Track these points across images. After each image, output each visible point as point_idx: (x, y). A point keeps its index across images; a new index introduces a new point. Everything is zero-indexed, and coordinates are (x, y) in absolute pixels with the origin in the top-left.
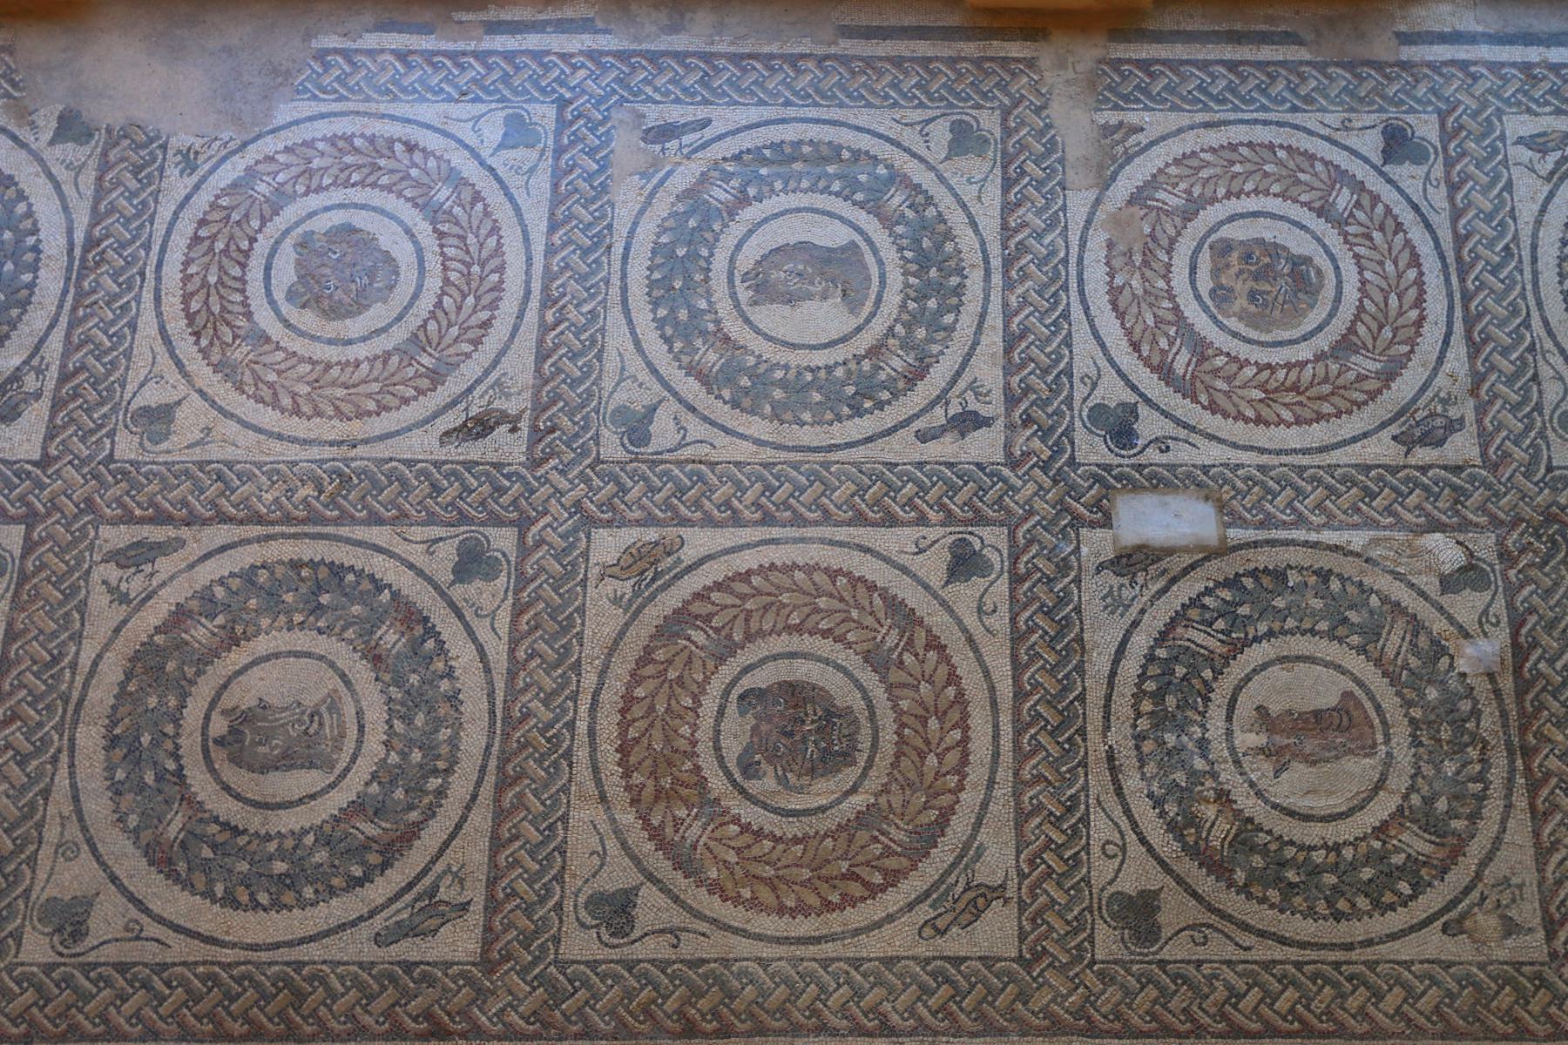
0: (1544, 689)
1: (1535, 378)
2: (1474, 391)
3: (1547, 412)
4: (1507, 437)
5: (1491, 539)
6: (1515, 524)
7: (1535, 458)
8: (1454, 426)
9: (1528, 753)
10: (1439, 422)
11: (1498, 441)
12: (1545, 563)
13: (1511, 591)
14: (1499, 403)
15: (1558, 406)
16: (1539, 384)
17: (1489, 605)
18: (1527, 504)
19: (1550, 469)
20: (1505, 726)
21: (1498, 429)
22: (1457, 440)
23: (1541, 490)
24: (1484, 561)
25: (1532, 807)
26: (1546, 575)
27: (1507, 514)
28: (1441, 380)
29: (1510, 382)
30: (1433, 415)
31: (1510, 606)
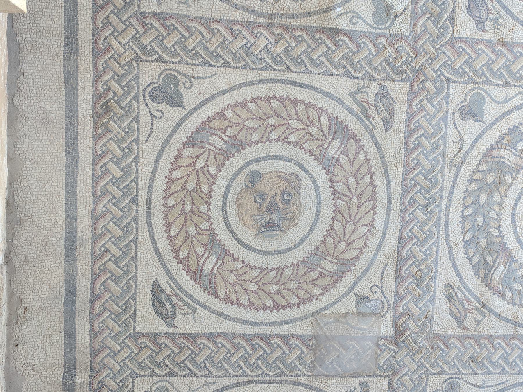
0: (309, 46)
1: (507, 84)
2: (501, 42)
3: (485, 87)
4: (471, 57)
5: (406, 32)
6: (414, 50)
7: (455, 72)
8: (480, 23)
9: (269, 26)
10: (484, 14)
11: (468, 51)
12: (388, 64)
13: (373, 38)
14: (493, 57)
15: (489, 95)
16: (503, 86)
17: (364, 21)
18: (427, 60)
19: (448, 80)
20: (287, 16)
21: (476, 52)
22: (472, 24)
23: (435, 72)
24: (392, 23)
25: (237, 22)
26: (381, 63)
27: (422, 46)
28: (510, 21)
29: (507, 67)
30: (488, 11)
31: (363, 35)
